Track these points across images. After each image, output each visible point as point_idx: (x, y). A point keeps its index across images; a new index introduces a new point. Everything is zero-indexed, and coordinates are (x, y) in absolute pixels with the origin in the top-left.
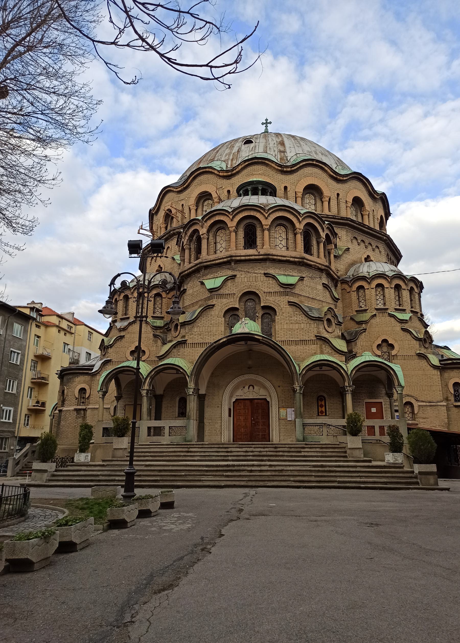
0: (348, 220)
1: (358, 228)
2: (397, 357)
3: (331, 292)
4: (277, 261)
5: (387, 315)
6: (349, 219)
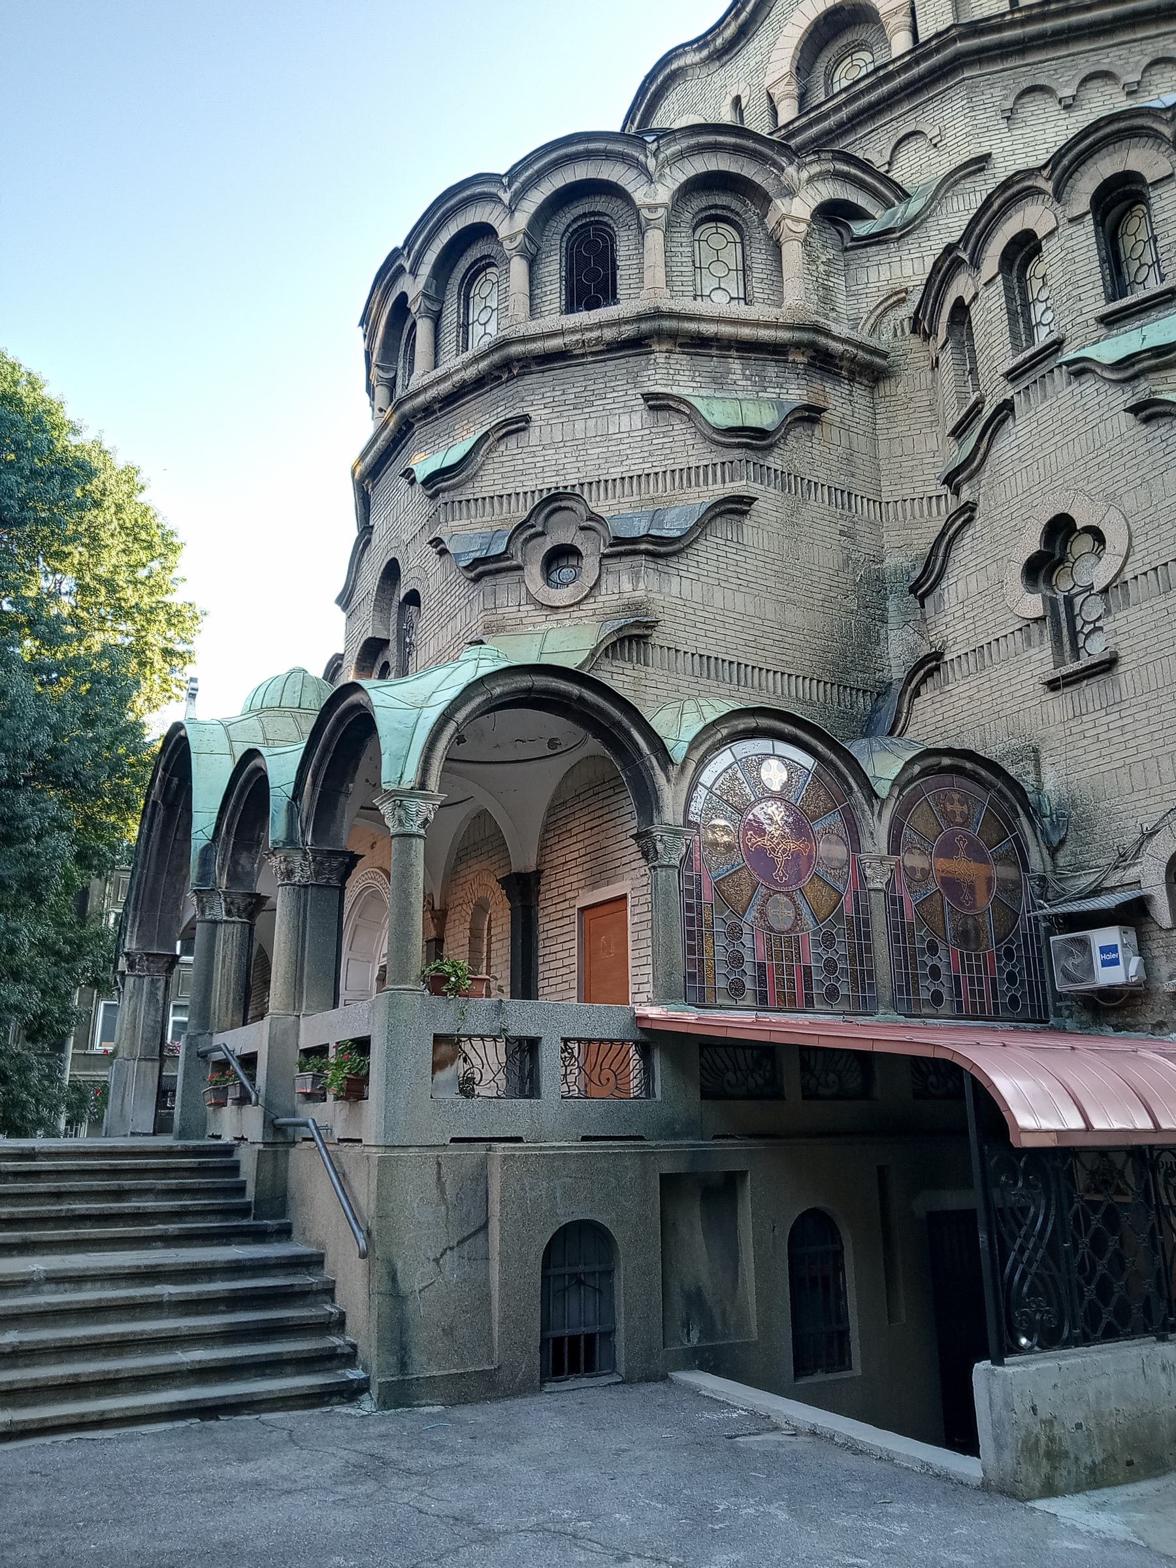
0: (954, 40)
1: (1041, 35)
2: (1127, 595)
3: (692, 415)
4: (441, 409)
5: (1060, 377)
6: (953, 32)
